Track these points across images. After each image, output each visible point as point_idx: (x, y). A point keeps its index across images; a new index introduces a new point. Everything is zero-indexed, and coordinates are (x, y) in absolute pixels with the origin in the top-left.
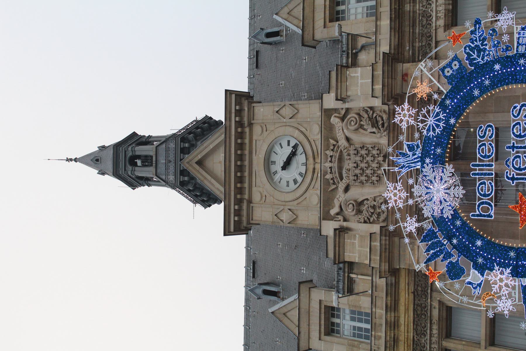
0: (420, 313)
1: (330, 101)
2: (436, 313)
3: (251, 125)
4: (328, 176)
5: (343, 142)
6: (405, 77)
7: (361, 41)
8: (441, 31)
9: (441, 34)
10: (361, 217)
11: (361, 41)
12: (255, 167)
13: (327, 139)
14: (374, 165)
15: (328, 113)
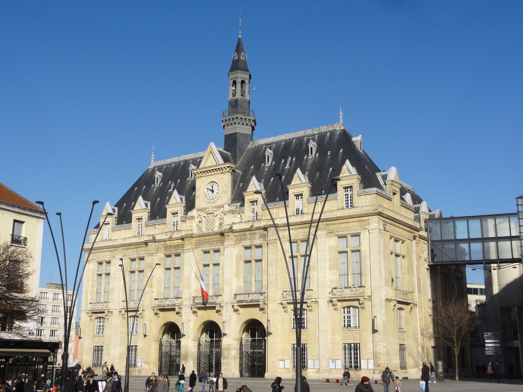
0: (177, 246)
1: (227, 208)
2: (178, 251)
3: (222, 173)
4: (207, 210)
5: (215, 214)
6: (228, 236)
7: (242, 215)
8: (242, 244)
9: (241, 244)
10: (198, 223)
11: (242, 215)
12: (211, 177)
13: (217, 207)
14: (210, 227)
15: (223, 207)
